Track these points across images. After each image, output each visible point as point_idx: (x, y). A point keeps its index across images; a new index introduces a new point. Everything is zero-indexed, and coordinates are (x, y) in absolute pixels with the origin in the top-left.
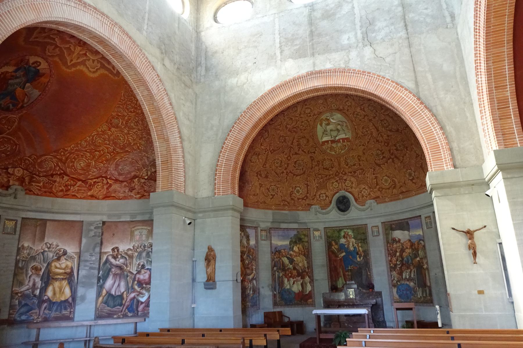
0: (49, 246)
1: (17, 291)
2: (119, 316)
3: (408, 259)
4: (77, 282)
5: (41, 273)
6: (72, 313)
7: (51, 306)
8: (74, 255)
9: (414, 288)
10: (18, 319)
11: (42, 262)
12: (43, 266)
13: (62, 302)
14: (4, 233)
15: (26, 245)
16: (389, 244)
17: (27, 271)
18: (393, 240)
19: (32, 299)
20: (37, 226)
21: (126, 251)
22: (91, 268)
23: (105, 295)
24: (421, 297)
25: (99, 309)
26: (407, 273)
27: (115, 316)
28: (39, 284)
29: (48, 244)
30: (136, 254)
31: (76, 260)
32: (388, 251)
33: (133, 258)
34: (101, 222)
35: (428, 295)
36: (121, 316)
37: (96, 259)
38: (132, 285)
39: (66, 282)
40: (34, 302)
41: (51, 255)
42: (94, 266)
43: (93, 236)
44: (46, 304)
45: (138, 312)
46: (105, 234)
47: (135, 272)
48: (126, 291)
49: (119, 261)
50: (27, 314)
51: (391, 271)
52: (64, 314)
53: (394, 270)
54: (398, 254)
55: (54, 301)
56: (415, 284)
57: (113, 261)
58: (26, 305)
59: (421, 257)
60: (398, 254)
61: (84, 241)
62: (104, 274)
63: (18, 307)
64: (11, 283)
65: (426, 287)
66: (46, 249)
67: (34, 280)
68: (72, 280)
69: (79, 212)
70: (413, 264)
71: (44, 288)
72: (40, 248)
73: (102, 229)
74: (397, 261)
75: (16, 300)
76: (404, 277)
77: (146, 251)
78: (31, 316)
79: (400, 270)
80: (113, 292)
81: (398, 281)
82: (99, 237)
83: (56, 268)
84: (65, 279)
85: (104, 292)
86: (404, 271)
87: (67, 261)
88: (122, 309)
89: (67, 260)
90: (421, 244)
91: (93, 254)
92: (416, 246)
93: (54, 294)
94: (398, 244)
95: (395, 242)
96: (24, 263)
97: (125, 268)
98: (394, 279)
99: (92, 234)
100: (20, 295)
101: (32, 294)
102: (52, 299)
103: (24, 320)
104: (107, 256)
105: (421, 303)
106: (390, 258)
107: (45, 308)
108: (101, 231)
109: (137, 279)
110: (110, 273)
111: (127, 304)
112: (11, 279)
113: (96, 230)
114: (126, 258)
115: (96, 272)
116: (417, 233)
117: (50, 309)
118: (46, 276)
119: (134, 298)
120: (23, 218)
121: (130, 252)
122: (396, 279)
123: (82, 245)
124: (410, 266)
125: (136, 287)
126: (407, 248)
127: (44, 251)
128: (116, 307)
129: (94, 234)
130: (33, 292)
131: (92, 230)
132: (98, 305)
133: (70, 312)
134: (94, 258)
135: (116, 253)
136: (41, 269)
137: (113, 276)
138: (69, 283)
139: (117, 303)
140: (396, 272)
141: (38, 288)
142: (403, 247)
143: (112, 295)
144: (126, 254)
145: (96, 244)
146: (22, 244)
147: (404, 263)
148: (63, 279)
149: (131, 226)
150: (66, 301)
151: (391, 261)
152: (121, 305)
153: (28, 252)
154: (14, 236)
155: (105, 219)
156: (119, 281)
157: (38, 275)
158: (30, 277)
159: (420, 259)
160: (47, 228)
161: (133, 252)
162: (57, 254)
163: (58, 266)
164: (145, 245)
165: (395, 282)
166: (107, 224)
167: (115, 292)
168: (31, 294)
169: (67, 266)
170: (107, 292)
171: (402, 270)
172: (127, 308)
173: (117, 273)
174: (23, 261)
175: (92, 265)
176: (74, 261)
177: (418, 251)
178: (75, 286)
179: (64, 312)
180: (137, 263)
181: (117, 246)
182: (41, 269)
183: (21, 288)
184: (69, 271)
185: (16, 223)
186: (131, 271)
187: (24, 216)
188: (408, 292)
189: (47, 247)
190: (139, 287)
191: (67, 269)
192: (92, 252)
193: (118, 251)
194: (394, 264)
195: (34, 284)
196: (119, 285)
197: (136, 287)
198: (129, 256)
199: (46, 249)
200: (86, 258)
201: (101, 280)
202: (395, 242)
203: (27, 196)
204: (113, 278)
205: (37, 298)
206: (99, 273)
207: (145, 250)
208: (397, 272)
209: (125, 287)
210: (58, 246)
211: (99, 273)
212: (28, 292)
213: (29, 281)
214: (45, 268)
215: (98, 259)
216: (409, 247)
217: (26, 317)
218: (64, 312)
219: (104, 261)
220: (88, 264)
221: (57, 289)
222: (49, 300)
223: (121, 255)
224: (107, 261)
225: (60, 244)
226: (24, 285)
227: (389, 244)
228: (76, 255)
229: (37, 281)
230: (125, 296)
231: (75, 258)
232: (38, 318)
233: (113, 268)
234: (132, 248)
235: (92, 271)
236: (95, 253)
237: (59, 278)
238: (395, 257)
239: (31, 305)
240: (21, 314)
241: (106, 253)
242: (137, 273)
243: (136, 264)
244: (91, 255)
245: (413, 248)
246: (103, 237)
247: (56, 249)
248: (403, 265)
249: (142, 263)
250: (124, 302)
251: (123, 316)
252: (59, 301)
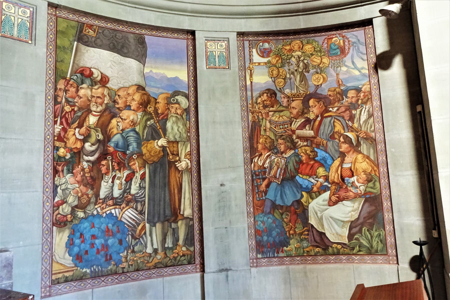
3: (125, 139)
9: (134, 228)
16: (61, 85)
18: (82, 73)
24: (156, 251)
26: (117, 182)
32: (56, 102)
35: (181, 242)
51: (56, 172)
53: (70, 171)
54: (92, 120)
56: (141, 213)
59: (172, 138)
60: (92, 120)
65: (176, 221)
70: (140, 155)
74: (84, 141)
76: (102, 195)
79: (91, 170)
81: (82, 206)
86: (107, 173)
90: (178, 103)
92: (161, 107)
94: (98, 91)
95: (88, 81)
98: (64, 202)
105: (155, 267)
106: (58, 128)
116: (170, 74)
122: (70, 199)
124: (131, 158)
126: (128, 107)
140: (74, 175)
142: (115, 102)
147: (111, 149)
151: (60, 138)
159: (169, 142)
165: (65, 209)
171: (100, 170)
177: (165, 119)
188: (110, 242)
194: (70, 150)
202: (88, 81)
208: (79, 178)
216: (134, 105)
227: (61, 85)
238: (80, 126)
245: (151, 109)
248: (104, 155)
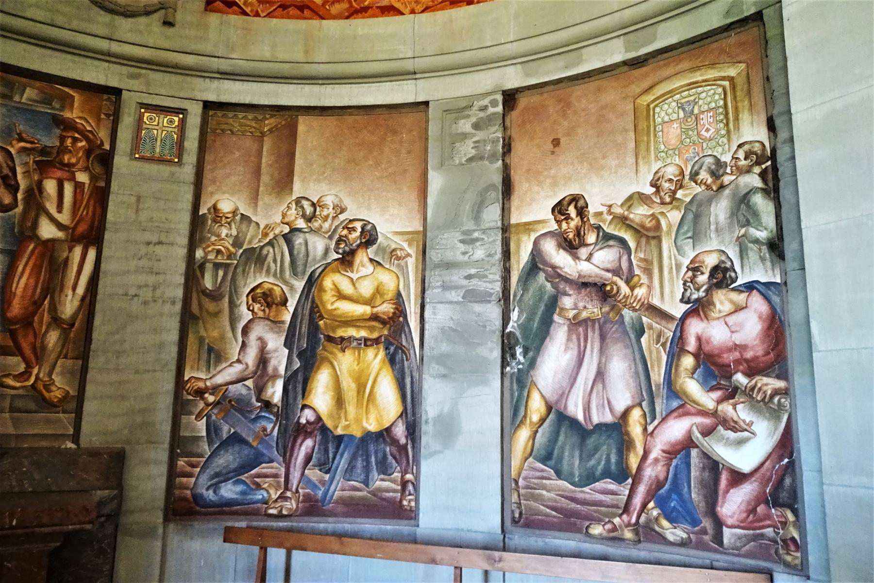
0: (309, 210)
1: (201, 385)
2: (614, 529)
4: (422, 359)
5: (287, 317)
6: (410, 487)
7: (331, 455)
8: (405, 245)
10: (210, 495)
11: (287, 273)
12: (292, 288)
13: (368, 437)
14: (142, 158)
15: (226, 206)
17: (233, 305)
19: (258, 418)
20: (263, 134)
21: (618, 211)
22: (472, 296)
23: (542, 421)
25: (521, 482)
27: (597, 530)
28: (280, 360)
29: (306, 204)
30: (675, 216)
31: (411, 262)
33: (659, 239)
34: (499, 98)
36: (628, 534)
37: (490, 255)
38: (668, 373)
39: (382, 354)
40: (265, 429)
41: (318, 245)
42: (481, 285)
43: (471, 160)
44: (309, 443)
45: (719, 524)
46: (519, 148)
47: (678, 310)
48: (640, 405)
49: (589, 259)
50: (243, 477)
52: (380, 490)
55: (339, 431)
57: (561, 259)
58: (236, 439)
61: (436, 181)
62: (530, 319)
63: (206, 449)
64: (174, 350)
66: (301, 224)
67: (262, 342)
68: (400, 347)
69: (409, 65)
71: (300, 378)
72: (278, 219)
73: (505, 128)
75: (199, 417)
77: (727, 192)
78: (258, 486)
80: (575, 409)
82: (492, 158)
83: (341, 296)
84: (377, 341)
85: (536, 407)
87: (379, 269)
88: (630, 497)
89: (379, 263)
91: (476, 235)
93: (339, 402)
96: (221, 273)
97: (625, 289)
99: (467, 149)
100: (211, 399)
101: (259, 400)
102: (329, 424)
103: (230, 503)
104: (536, 243)
107: (308, 459)
108: (500, 135)
109: (692, 345)
110: (556, 317)
111: (649, 473)
112: (173, 336)
113: (480, 135)
114: (622, 242)
115: (494, 312)
117: (325, 466)
118: (305, 329)
119: (688, 444)
120: (208, 105)
121: (640, 213)
123: (430, 201)
125: (693, 387)
127: (294, 230)
128: (598, 485)
129: (473, 152)
130: (260, 389)
131: (464, 136)
132: (515, 463)
133: (404, 484)
134: (479, 253)
135: (575, 221)
136: (284, 302)
137: (570, 330)
138: (392, 360)
139: (598, 462)
141: (275, 376)
143: (573, 422)
144: (623, 221)
145: (487, 189)
146: (210, 205)
148: (367, 342)
149: (636, 89)
150: (385, 434)
152: (621, 474)
153: (234, 232)
154: (174, 169)
155: (513, 79)
156: (602, 351)
157: (276, 323)
158: (245, 331)
160: (298, 141)
161: (657, 210)
162: (340, 240)
163: (346, 287)
164: (718, 162)
166: (523, 102)
167: (587, 409)
168: (254, 400)
169: (378, 291)
170: (549, 408)
172: (651, 495)
173: (584, 315)
174: (217, 266)
175: (475, 281)
176: (404, 270)
178: (416, 374)
179: (379, 482)
180: (686, 262)
181: (575, 190)
182: (286, 300)
183: (213, 372)
184: (386, 308)
185: (183, 122)
186: (656, 301)
187: (212, 97)
189: (304, 216)
190: (712, 389)
191: (378, 301)
192: (470, 225)
193: (581, 212)
195: (263, 360)
196: (600, 375)
197: (693, 387)
198: (639, 231)
199: (301, 224)
200: (449, 256)
201: (519, 350)
203: (214, 19)
204: (569, 339)
205: (277, 415)
206: (506, 319)
207: (722, 187)
209: (632, 384)
210: (343, 211)
211: (506, 319)
212: (237, 389)
213: (244, 345)
214: (298, 296)
215: (499, 255)
217: (240, 488)
218: (379, 482)
219: (521, 267)
220: (456, 277)
221: (349, 385)
222: (319, 427)
223: (598, 228)
224: (536, 263)
225: (347, 202)
226: (227, 359)
228: (410, 245)
229: (270, 346)
230: (635, 429)
231: (409, 255)
232: (282, 497)
233: (565, 294)
234: (649, 190)
235: (477, 308)
236: (484, 231)
237: (350, 339)
239: (255, 444)
240: (217, 475)
241: (528, 227)
242: (686, 315)
243: (678, 266)
244: (469, 241)
246: (514, 159)
247: (336, 223)
249: (711, 261)
250: (633, 462)
251: (637, 533)
252: (358, 434)
